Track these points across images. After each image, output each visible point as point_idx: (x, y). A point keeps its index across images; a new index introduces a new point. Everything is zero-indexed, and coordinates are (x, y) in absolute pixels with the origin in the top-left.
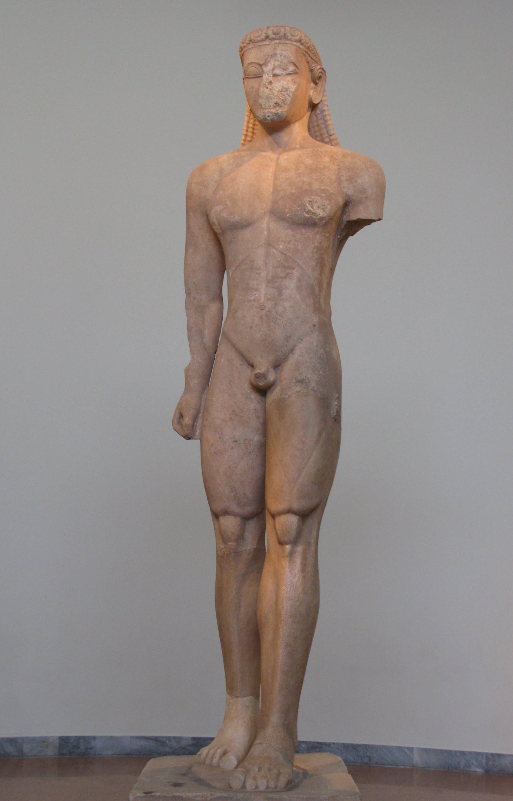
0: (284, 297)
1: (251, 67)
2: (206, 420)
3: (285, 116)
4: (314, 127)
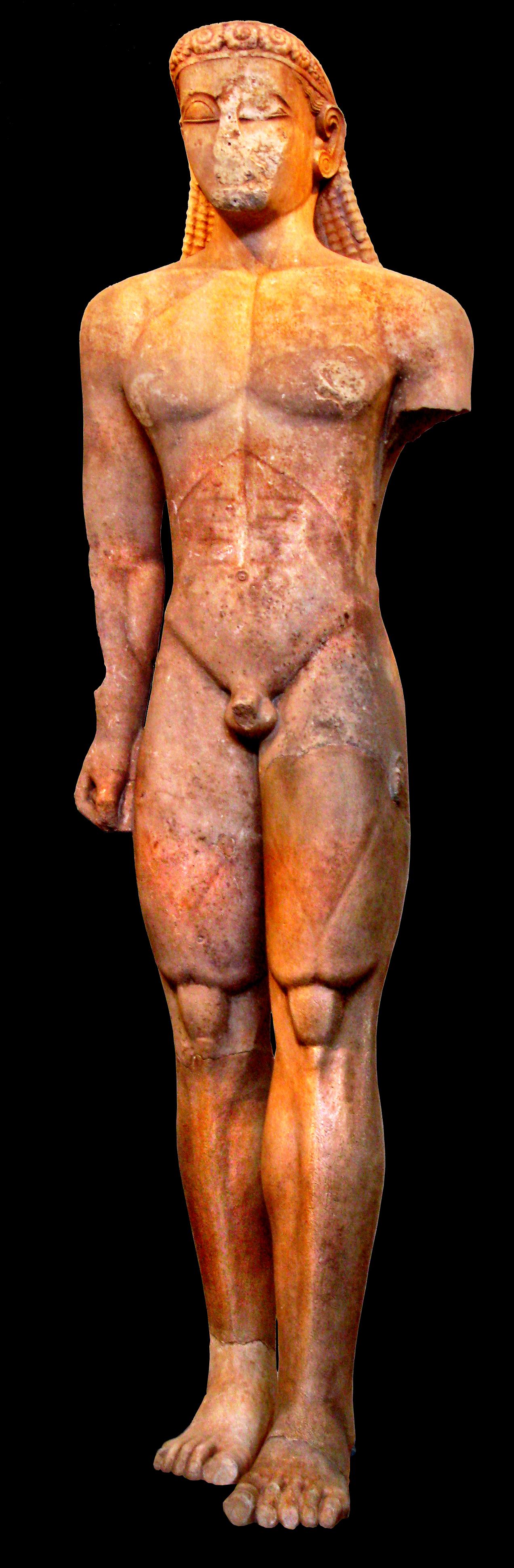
0: (283, 557)
1: (196, 101)
2: (142, 796)
3: (267, 200)
4: (325, 224)
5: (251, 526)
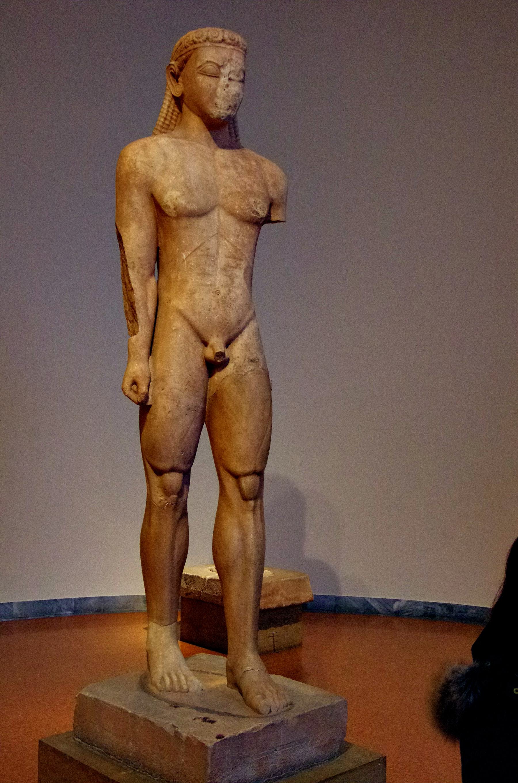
0: (234, 285)
1: (210, 65)
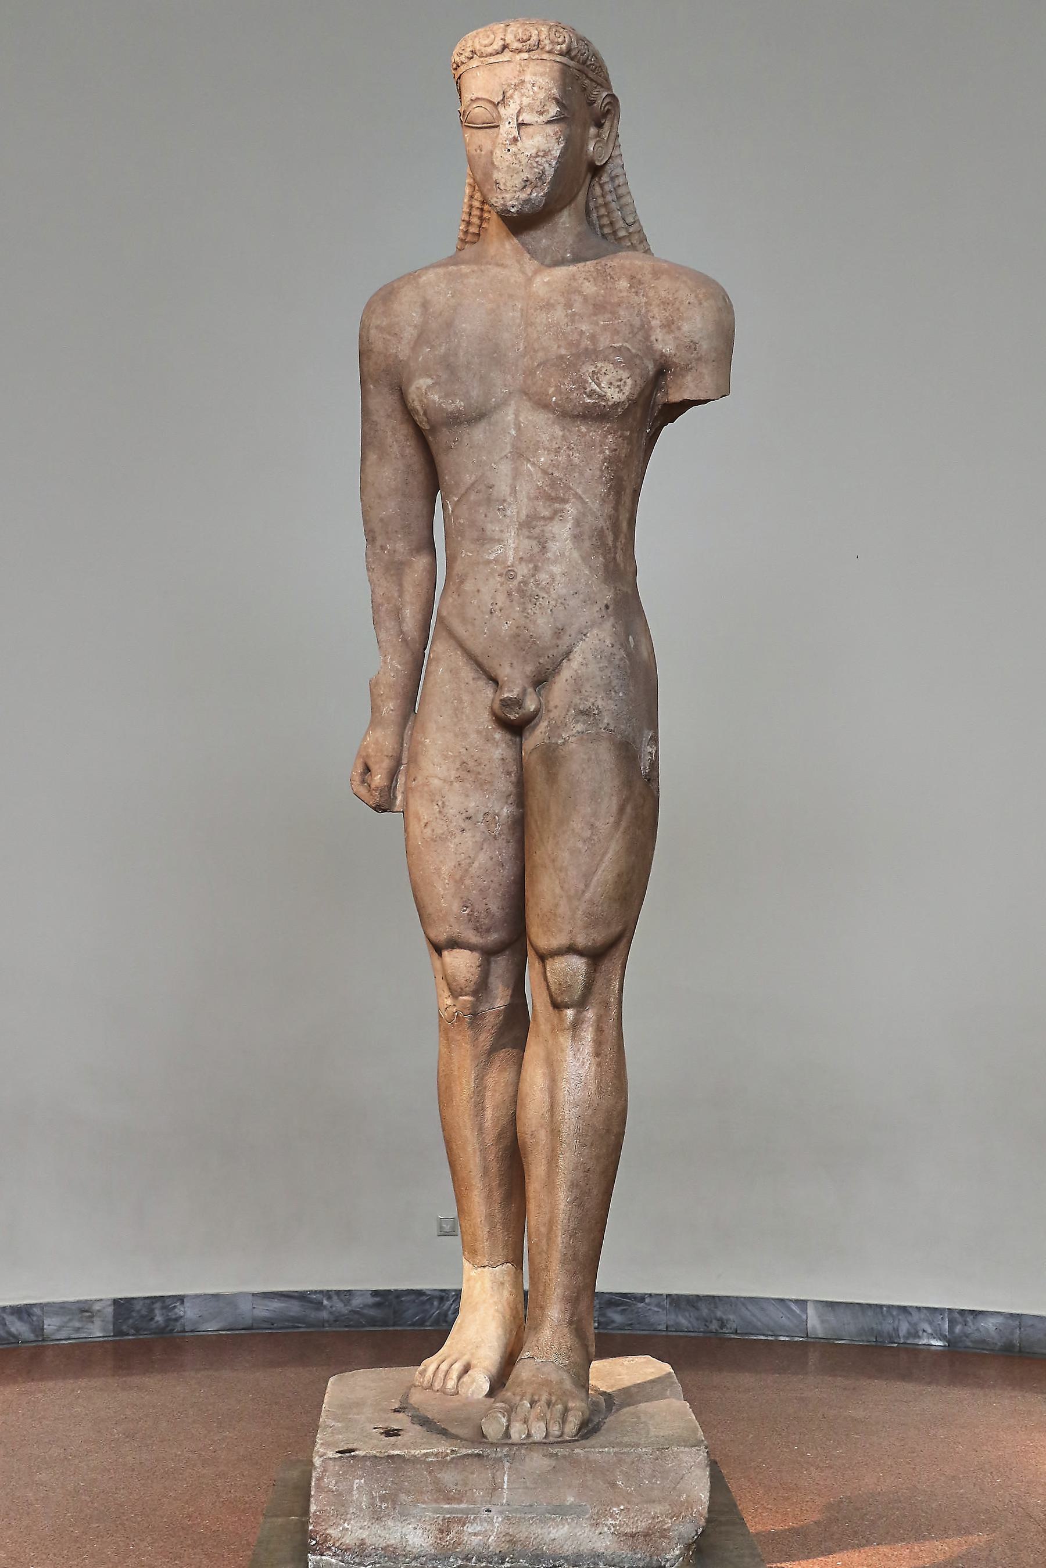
5: (521, 526)
